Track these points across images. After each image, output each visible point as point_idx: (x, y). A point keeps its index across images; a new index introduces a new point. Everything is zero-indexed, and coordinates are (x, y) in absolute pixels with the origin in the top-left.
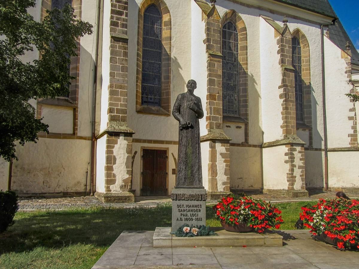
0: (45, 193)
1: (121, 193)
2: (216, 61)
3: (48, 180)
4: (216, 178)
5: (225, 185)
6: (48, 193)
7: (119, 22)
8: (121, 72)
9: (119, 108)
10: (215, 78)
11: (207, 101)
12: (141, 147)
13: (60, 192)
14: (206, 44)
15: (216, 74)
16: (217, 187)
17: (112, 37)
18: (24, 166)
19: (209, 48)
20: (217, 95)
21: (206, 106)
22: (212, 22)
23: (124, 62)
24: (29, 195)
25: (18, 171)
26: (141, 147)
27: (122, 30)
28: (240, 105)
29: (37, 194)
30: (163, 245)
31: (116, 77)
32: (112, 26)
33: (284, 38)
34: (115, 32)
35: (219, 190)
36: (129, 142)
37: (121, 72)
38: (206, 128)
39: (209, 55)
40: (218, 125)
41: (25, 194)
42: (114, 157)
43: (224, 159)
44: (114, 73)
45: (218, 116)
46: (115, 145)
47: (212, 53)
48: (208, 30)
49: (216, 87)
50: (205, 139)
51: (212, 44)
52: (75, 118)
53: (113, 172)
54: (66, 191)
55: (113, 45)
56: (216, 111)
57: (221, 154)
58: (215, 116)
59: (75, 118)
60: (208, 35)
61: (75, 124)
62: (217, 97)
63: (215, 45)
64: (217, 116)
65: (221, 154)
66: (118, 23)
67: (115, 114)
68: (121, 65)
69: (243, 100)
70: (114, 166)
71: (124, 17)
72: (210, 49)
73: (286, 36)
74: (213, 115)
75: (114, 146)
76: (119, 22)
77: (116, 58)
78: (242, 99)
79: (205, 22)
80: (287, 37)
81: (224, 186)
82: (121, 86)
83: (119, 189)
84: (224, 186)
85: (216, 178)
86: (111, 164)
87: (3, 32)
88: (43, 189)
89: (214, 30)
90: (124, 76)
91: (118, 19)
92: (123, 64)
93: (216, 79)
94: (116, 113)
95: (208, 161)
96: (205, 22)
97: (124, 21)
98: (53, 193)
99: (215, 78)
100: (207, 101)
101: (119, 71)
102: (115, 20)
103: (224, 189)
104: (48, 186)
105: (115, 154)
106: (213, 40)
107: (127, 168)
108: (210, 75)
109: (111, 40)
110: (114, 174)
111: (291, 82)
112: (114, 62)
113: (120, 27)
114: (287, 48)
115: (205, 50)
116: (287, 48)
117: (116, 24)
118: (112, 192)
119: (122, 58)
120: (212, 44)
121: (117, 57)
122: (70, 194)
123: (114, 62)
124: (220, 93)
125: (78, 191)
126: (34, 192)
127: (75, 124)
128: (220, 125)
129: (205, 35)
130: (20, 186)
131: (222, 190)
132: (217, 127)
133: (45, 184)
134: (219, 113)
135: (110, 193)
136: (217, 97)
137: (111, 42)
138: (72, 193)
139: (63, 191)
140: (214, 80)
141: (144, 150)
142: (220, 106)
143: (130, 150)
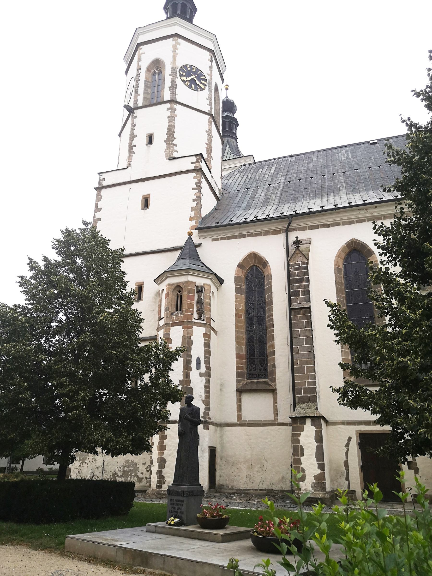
0: (249, 490)
1: (313, 493)
3: (251, 474)
6: (253, 490)
7: (300, 290)
9: (306, 387)
12: (357, 431)
13: (264, 489)
18: (228, 459)
23: (307, 334)
24: (233, 491)
25: (223, 463)
26: (357, 431)
27: (304, 298)
29: (241, 490)
30: (14, 549)
36: (316, 428)
41: (230, 489)
42: (301, 446)
44: (298, 348)
46: (302, 433)
52: (275, 402)
53: (302, 466)
54: (270, 489)
59: (275, 402)
61: (276, 409)
67: (303, 395)
70: (302, 459)
71: (305, 283)
75: (300, 434)
76: (300, 290)
82: (307, 361)
83: (311, 488)
86: (299, 456)
87: (44, 362)
88: (247, 484)
90: (309, 348)
91: (298, 287)
92: (307, 336)
94: (304, 394)
98: (257, 490)
101: (303, 345)
104: (251, 482)
105: (301, 444)
107: (317, 461)
110: (302, 468)
118: (302, 491)
122: (274, 492)
123: (296, 336)
125: (284, 489)
126: (238, 488)
127: (276, 409)
130: (226, 480)
133: (248, 479)
135: (300, 492)
138: (276, 491)
139: (267, 488)
141: (360, 435)
143: (319, 438)
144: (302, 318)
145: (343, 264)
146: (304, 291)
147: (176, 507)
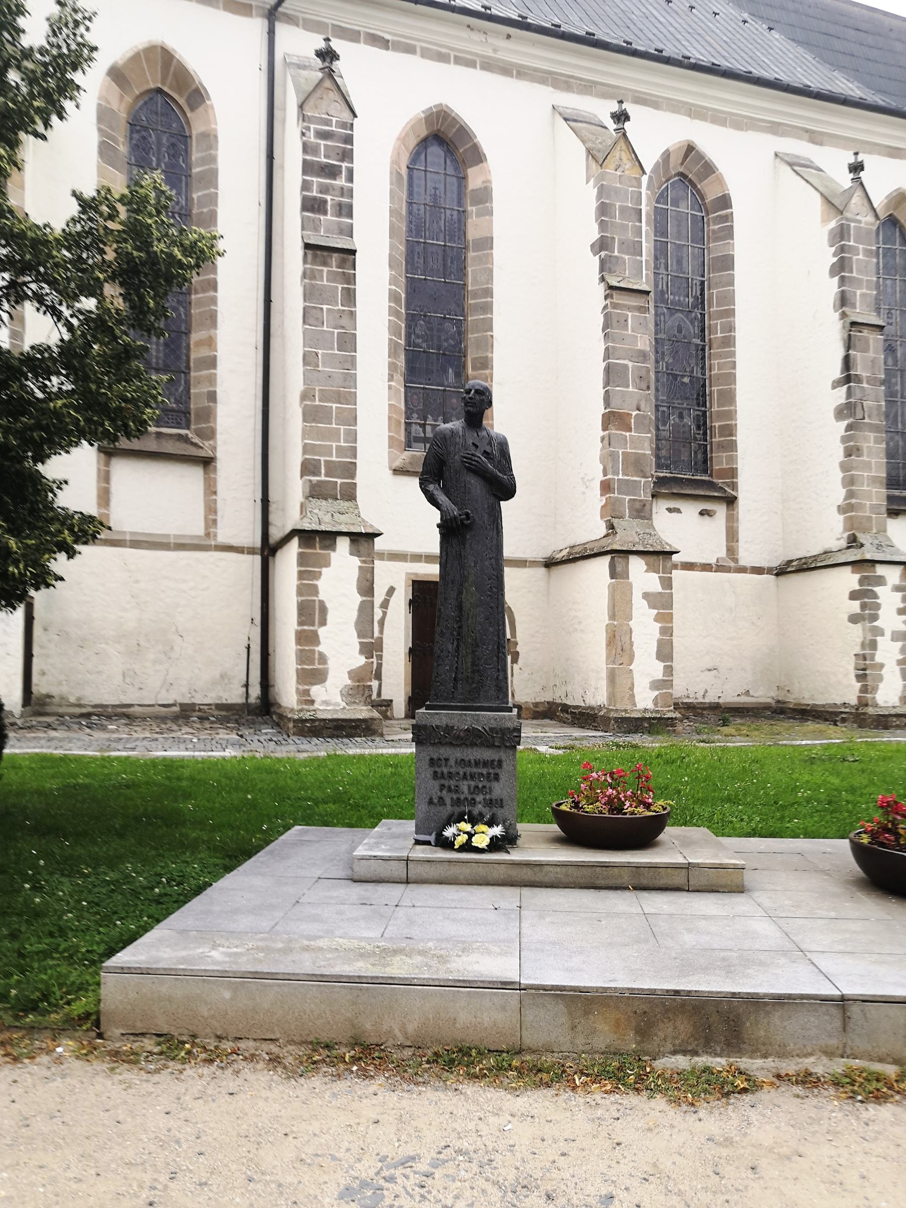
1: (344, 708)
2: (629, 308)
4: (631, 667)
5: (658, 690)
8: (337, 352)
9: (334, 459)
10: (626, 362)
11: (602, 433)
12: (407, 574)
14: (598, 256)
15: (630, 349)
16: (633, 696)
17: (307, 246)
19: (604, 266)
20: (634, 413)
21: (601, 450)
22: (618, 185)
23: (344, 321)
26: (407, 574)
27: (339, 223)
28: (711, 443)
31: (323, 366)
32: (308, 211)
33: (853, 224)
34: (316, 229)
35: (641, 705)
37: (337, 352)
38: (602, 517)
39: (608, 292)
40: (638, 505)
42: (322, 603)
43: (656, 611)
45: (638, 479)
46: (324, 570)
47: (617, 285)
48: (603, 210)
49: (631, 389)
50: (595, 551)
51: (616, 253)
52: (211, 489)
53: (320, 648)
55: (312, 270)
56: (635, 464)
57: (646, 596)
58: (627, 480)
60: (603, 225)
61: (211, 509)
62: (633, 421)
63: (627, 257)
64: (635, 478)
65: (646, 596)
66: (325, 202)
67: (323, 478)
68: (336, 331)
69: (719, 426)
70: (322, 632)
71: (341, 182)
72: (610, 271)
73: (859, 217)
74: (621, 477)
75: (320, 573)
76: (329, 198)
77: (322, 309)
78: (717, 424)
79: (594, 187)
80: (860, 222)
81: (657, 693)
83: (338, 699)
84: (657, 693)
85: (631, 667)
86: (313, 625)
89: (623, 209)
90: (346, 361)
91: (324, 189)
92: (343, 327)
93: (630, 364)
94: (326, 476)
95: (607, 617)
96: (594, 187)
97: (342, 195)
99: (626, 362)
100: (602, 433)
101: (332, 349)
102: (315, 194)
103: (655, 701)
106: (622, 243)
107: (359, 637)
108: (608, 354)
109: (305, 255)
110: (320, 654)
111: (873, 367)
112: (315, 323)
113: (332, 216)
114: (861, 257)
115: (597, 276)
116: (861, 257)
117: (319, 206)
118: (316, 706)
119: (339, 310)
120: (616, 253)
121: (325, 307)
123: (316, 323)
124: (643, 407)
125: (224, 702)
127: (211, 509)
128: (644, 505)
129: (596, 227)
131: (650, 706)
132: (634, 513)
134: (642, 471)
135: (312, 708)
136: (633, 421)
137: (305, 261)
140: (626, 366)
142: (643, 449)
143: (368, 584)
144: (332, 277)
145: (408, 167)
146: (340, 205)
147: (464, 786)
